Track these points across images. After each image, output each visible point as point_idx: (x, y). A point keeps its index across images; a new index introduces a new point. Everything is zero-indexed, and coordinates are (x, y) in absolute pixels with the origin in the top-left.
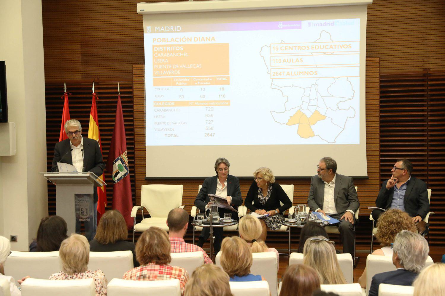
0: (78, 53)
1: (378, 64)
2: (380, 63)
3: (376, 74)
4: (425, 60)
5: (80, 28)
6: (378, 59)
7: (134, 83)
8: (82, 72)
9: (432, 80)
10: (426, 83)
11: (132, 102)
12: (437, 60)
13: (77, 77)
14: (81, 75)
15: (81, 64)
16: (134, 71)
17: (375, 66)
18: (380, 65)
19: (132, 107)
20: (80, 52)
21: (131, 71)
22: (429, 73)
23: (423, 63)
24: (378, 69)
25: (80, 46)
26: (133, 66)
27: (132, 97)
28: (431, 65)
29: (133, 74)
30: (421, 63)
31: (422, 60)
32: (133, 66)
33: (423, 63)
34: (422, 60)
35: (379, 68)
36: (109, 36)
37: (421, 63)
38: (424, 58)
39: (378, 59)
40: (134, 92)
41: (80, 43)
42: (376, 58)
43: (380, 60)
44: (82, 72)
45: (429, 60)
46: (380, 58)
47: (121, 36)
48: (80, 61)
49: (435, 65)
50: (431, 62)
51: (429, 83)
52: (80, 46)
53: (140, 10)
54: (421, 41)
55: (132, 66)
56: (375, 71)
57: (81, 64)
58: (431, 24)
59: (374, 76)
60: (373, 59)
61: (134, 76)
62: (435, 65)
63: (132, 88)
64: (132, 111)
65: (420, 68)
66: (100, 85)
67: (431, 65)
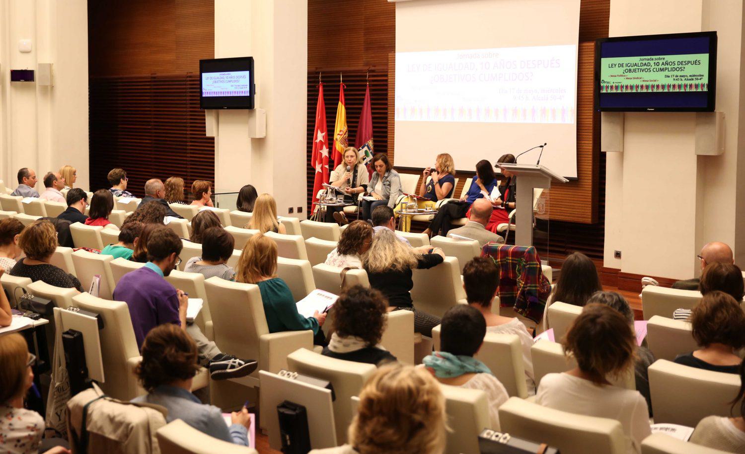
5: (363, 16)
6: (593, 44)
7: (389, 71)
11: (387, 90)
13: (359, 66)
14: (363, 62)
15: (363, 51)
19: (387, 95)
25: (363, 34)
26: (389, 54)
27: (387, 85)
39: (593, 44)
40: (389, 80)
44: (364, 60)
63: (387, 76)
64: (387, 99)
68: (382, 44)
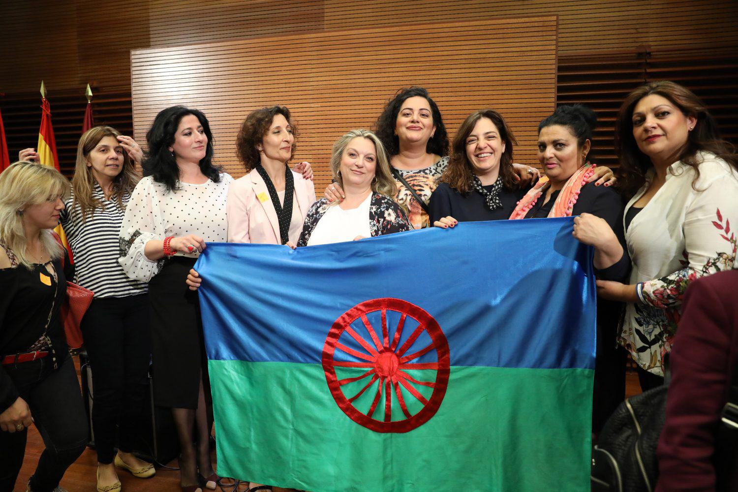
3: (549, 47)
4: (640, 30)
6: (555, 17)
8: (80, 75)
9: (652, 65)
10: (644, 71)
12: (663, 30)
17: (549, 33)
22: (648, 51)
23: (636, 36)
28: (651, 39)
30: (632, 36)
31: (634, 31)
33: (636, 36)
34: (634, 31)
37: (632, 36)
38: (638, 26)
39: (555, 18)
43: (557, 20)
44: (80, 75)
45: (648, 31)
49: (659, 38)
50: (651, 34)
51: (648, 71)
56: (548, 43)
59: (547, 52)
60: (545, 19)
62: (659, 38)
65: (629, 45)
66: (106, 92)
67: (651, 39)
68: (113, 47)
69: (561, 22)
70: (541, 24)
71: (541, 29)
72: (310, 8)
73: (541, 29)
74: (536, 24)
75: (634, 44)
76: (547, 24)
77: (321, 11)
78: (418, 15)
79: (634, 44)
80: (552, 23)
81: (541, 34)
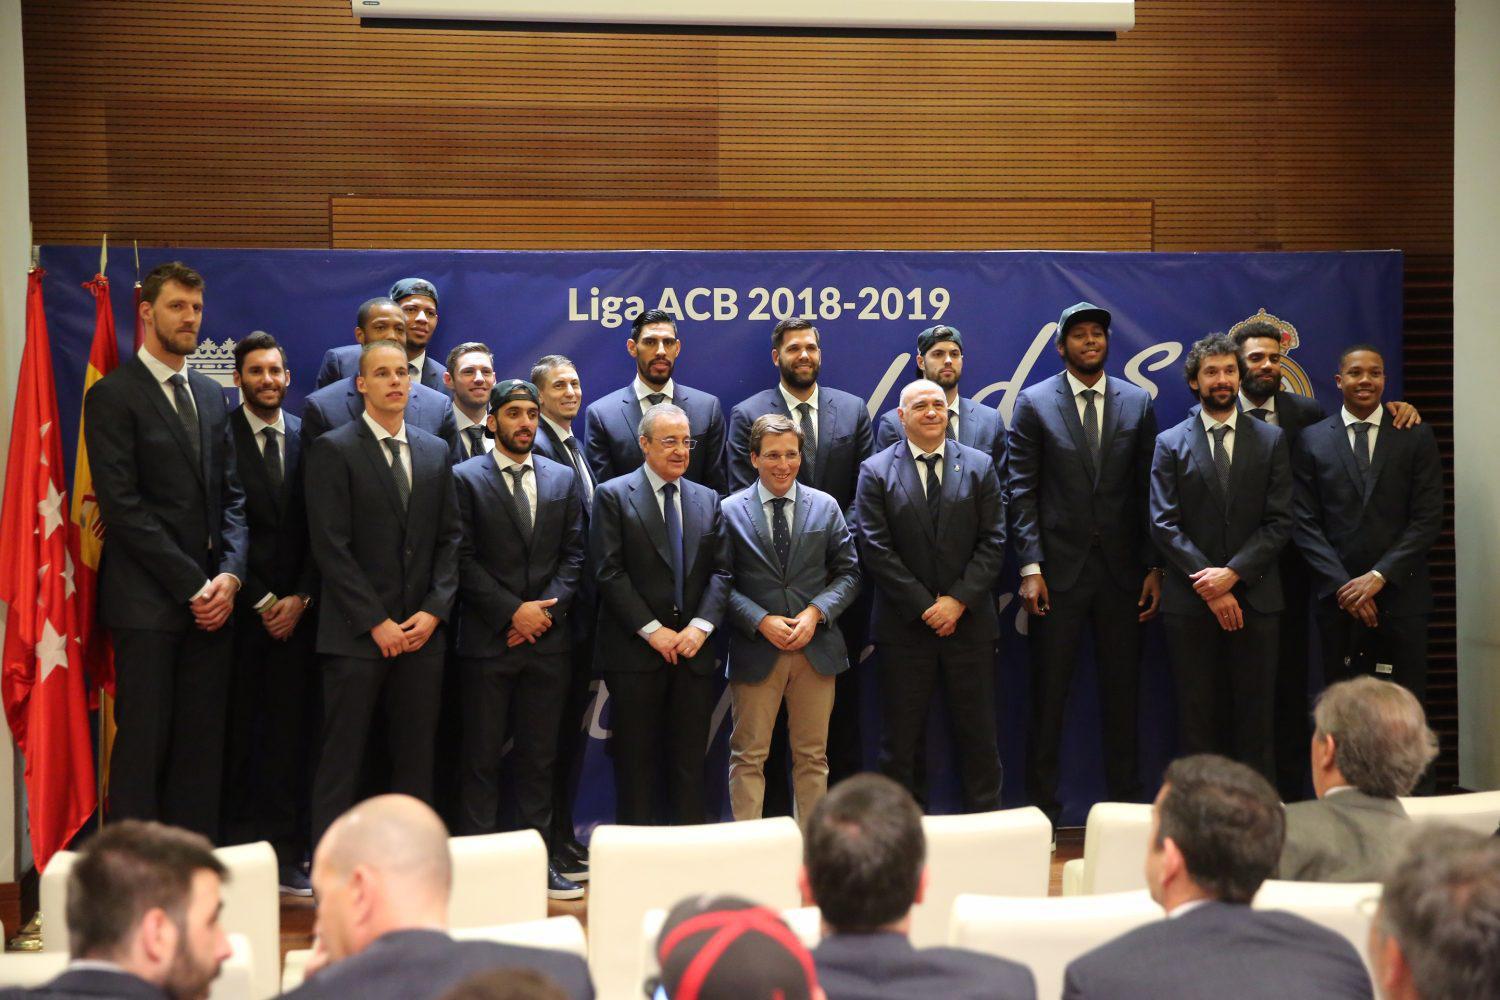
0: (95, 145)
1: (1148, 222)
2: (1152, 218)
4: (1263, 216)
16: (335, 218)
18: (1152, 225)
20: (104, 145)
21: (326, 221)
24: (1150, 236)
25: (103, 121)
26: (335, 201)
29: (331, 232)
31: (1252, 216)
32: (335, 201)
34: (1252, 216)
35: (1152, 233)
36: (218, 91)
39: (1149, 204)
41: (102, 112)
42: (1141, 204)
43: (1153, 209)
46: (1153, 202)
47: (266, 91)
48: (104, 178)
52: (103, 121)
53: (364, 3)
54: (1251, 156)
55: (330, 201)
56: (1138, 244)
57: (105, 187)
58: (1280, 104)
61: (335, 235)
69: (1157, 209)
70: (1127, 214)
71: (1129, 221)
72: (688, 131)
73: (1129, 221)
74: (1120, 213)
75: (1253, 239)
76: (1137, 214)
77: (709, 139)
78: (897, 163)
79: (1253, 239)
80: (1145, 214)
81: (1127, 230)
